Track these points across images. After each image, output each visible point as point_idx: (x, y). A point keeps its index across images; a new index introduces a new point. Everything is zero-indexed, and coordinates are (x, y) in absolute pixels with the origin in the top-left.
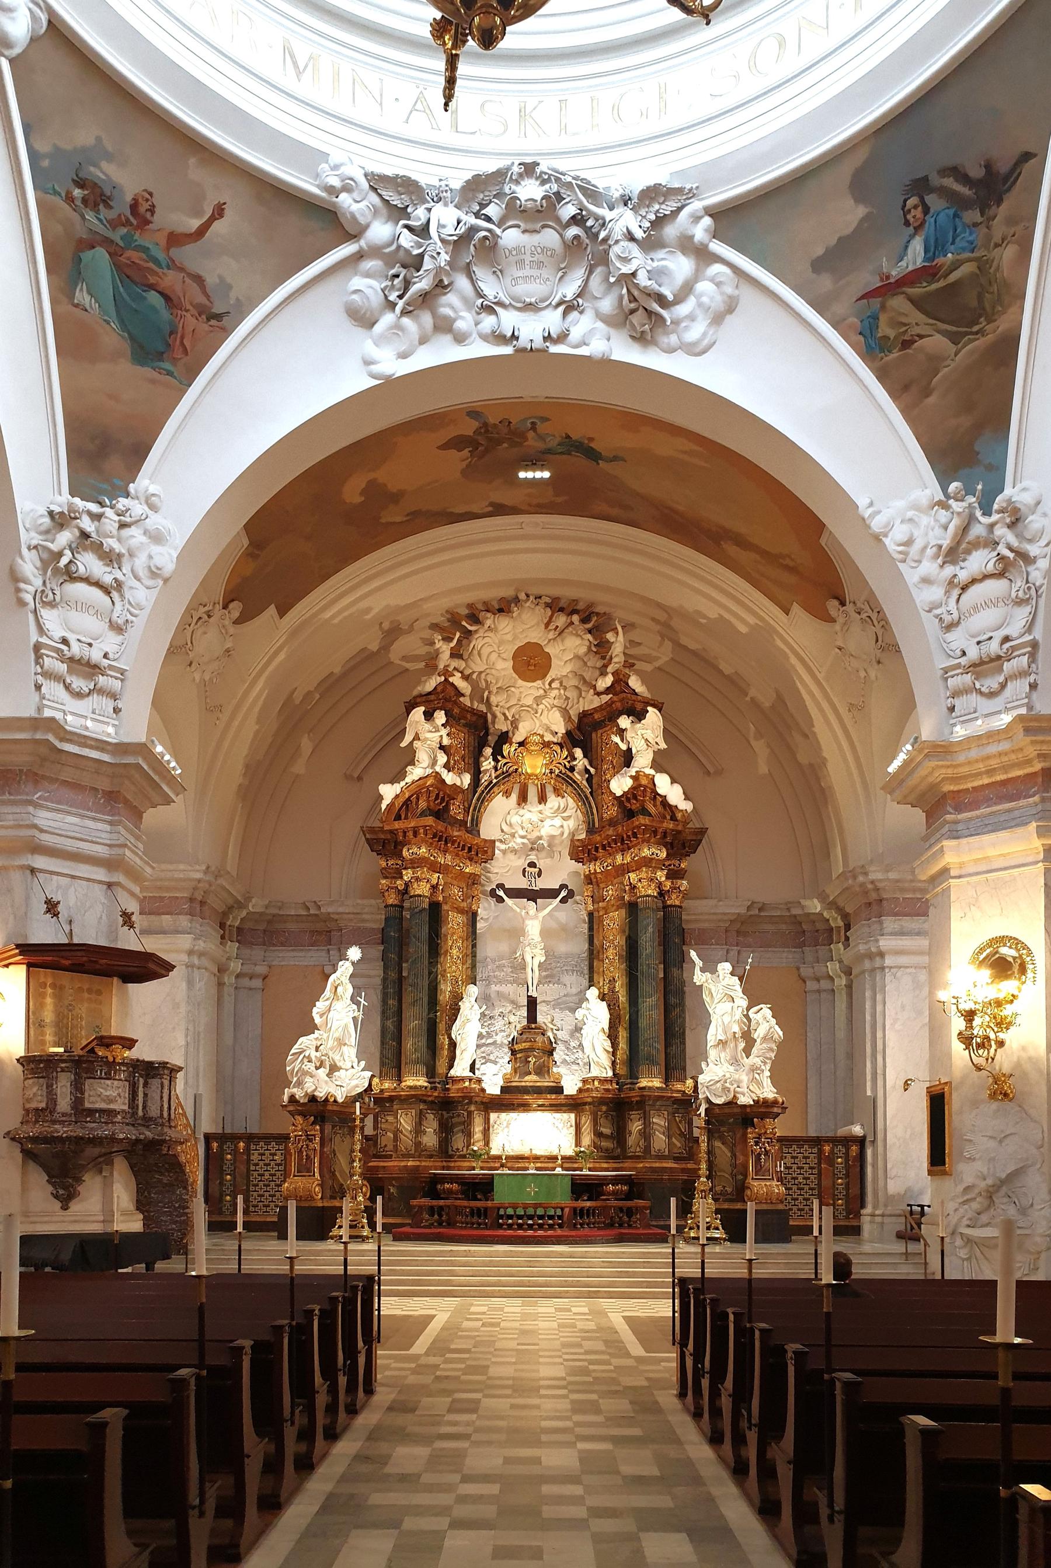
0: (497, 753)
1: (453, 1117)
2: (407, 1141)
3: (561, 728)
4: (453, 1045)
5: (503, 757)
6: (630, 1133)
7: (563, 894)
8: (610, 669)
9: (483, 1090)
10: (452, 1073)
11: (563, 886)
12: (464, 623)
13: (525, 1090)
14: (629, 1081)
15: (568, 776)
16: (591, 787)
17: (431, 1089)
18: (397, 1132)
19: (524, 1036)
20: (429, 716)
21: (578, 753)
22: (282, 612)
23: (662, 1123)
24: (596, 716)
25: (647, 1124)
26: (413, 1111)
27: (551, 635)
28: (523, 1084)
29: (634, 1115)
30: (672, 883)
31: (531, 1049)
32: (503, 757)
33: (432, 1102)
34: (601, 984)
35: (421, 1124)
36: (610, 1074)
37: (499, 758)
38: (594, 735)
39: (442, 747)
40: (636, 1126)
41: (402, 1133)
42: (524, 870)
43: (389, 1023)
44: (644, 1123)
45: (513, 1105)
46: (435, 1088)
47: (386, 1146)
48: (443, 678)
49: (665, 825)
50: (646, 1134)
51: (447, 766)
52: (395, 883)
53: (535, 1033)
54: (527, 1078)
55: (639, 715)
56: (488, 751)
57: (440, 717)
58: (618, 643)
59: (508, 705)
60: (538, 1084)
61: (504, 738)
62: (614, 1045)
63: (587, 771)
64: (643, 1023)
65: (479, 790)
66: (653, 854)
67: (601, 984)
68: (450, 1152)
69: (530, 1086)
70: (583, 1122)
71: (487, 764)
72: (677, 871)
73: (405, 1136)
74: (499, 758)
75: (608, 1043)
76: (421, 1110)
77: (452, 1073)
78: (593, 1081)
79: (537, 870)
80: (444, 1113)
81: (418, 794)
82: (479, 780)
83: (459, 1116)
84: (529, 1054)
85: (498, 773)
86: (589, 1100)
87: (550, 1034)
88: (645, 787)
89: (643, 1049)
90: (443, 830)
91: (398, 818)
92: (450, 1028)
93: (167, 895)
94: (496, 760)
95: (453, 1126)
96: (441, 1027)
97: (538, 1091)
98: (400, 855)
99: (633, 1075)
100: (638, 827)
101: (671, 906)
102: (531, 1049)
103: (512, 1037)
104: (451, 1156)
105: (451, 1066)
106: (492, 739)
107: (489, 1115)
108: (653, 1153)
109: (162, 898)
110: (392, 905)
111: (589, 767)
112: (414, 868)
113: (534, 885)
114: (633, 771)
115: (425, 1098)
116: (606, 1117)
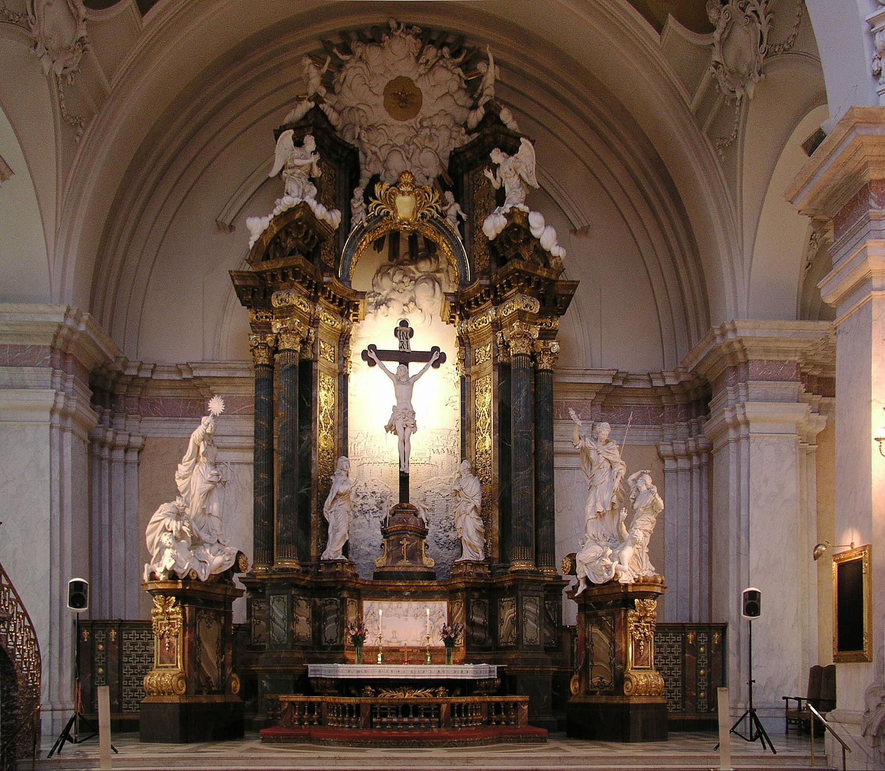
0: (369, 193)
1: (325, 605)
2: (279, 629)
3: (434, 171)
4: (325, 524)
5: (375, 198)
6: (502, 621)
8: (483, 101)
9: (356, 576)
10: (325, 556)
12: (335, 51)
13: (398, 576)
14: (502, 565)
15: (440, 222)
16: (463, 235)
17: (304, 572)
18: (270, 619)
19: (397, 516)
21: (449, 195)
23: (533, 610)
24: (468, 155)
25: (520, 612)
26: (285, 596)
27: (422, 70)
28: (396, 569)
29: (506, 601)
30: (544, 343)
31: (404, 531)
32: (375, 198)
33: (304, 588)
34: (473, 458)
35: (293, 612)
36: (482, 558)
37: (371, 199)
38: (465, 178)
39: (311, 179)
40: (508, 614)
41: (274, 620)
43: (260, 499)
44: (517, 611)
45: (386, 591)
46: (306, 573)
47: (260, 635)
48: (312, 104)
49: (539, 272)
50: (518, 622)
51: (317, 198)
52: (265, 339)
53: (407, 512)
54: (400, 563)
55: (511, 150)
56: (358, 192)
57: (310, 143)
58: (490, 73)
59: (379, 144)
60: (411, 569)
61: (375, 179)
62: (486, 524)
63: (459, 217)
64: (515, 500)
66: (526, 306)
67: (473, 458)
68: (324, 644)
69: (403, 572)
70: (455, 610)
71: (357, 204)
72: (548, 330)
73: (278, 624)
74: (371, 199)
75: (480, 524)
76: (292, 595)
77: (325, 556)
78: (466, 564)
79: (409, 329)
80: (317, 600)
81: (286, 230)
82: (350, 224)
83: (331, 603)
84: (402, 536)
86: (462, 586)
87: (422, 515)
88: (519, 226)
89: (516, 528)
90: (313, 273)
91: (266, 257)
92: (321, 505)
93: (29, 343)
94: (368, 202)
95: (327, 614)
96: (314, 503)
97: (409, 576)
98: (268, 306)
99: (505, 559)
100: (512, 273)
101: (542, 370)
102: (404, 531)
103: (384, 517)
104: (325, 648)
105: (324, 548)
106: (364, 182)
107: (362, 603)
108: (525, 643)
109: (23, 347)
110: (262, 365)
111: (460, 213)
112: (283, 317)
113: (406, 347)
114: (507, 208)
115: (297, 582)
116: (479, 604)
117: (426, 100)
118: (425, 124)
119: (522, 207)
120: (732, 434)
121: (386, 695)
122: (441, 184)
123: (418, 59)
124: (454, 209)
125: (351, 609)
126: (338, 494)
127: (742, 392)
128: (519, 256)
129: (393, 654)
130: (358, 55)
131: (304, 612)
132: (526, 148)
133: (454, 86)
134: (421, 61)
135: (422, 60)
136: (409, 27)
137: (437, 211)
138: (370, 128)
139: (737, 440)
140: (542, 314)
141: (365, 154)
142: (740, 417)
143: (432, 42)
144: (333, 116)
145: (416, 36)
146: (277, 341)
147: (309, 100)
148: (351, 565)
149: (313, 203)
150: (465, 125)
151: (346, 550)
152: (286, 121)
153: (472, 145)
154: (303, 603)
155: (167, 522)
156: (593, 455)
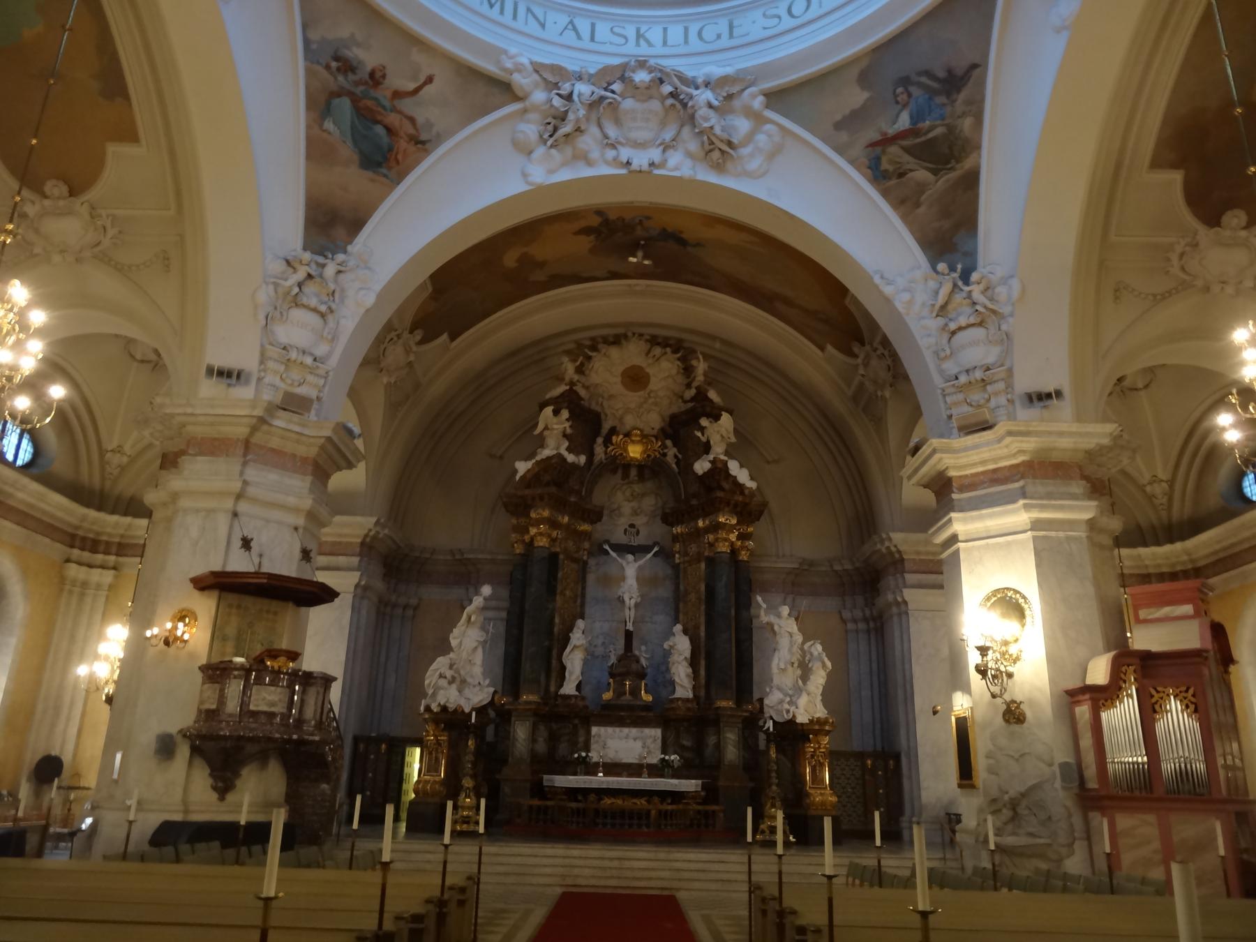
0: (607, 441)
4: (563, 668)
5: (612, 444)
7: (656, 549)
11: (655, 544)
20: (556, 412)
21: (669, 443)
22: (453, 338)
32: (612, 444)
37: (609, 445)
39: (565, 435)
41: (517, 740)
42: (626, 530)
48: (568, 388)
50: (718, 746)
51: (569, 450)
55: (717, 418)
56: (600, 440)
57: (565, 414)
60: (632, 703)
61: (613, 431)
65: (593, 467)
71: (599, 450)
74: (609, 445)
85: (607, 456)
91: (528, 486)
96: (555, 652)
97: (630, 708)
98: (528, 516)
105: (561, 686)
111: (677, 454)
114: (711, 457)
117: (653, 380)
118: (652, 395)
119: (723, 457)
120: (895, 610)
121: (608, 801)
122: (664, 434)
123: (647, 354)
124: (672, 451)
125: (582, 732)
126: (575, 647)
127: (900, 581)
128: (722, 489)
129: (613, 768)
130: (603, 352)
131: (543, 733)
132: (726, 419)
133: (674, 371)
134: (649, 356)
135: (651, 355)
136: (641, 335)
137: (659, 453)
138: (611, 397)
139: (900, 615)
140: (739, 523)
141: (606, 415)
142: (899, 599)
143: (658, 344)
144: (582, 393)
145: (647, 341)
146: (532, 539)
147: (566, 385)
148: (583, 698)
149: (566, 454)
150: (682, 397)
151: (579, 688)
152: (548, 396)
153: (687, 412)
154: (542, 728)
155: (442, 670)
156: (776, 628)
